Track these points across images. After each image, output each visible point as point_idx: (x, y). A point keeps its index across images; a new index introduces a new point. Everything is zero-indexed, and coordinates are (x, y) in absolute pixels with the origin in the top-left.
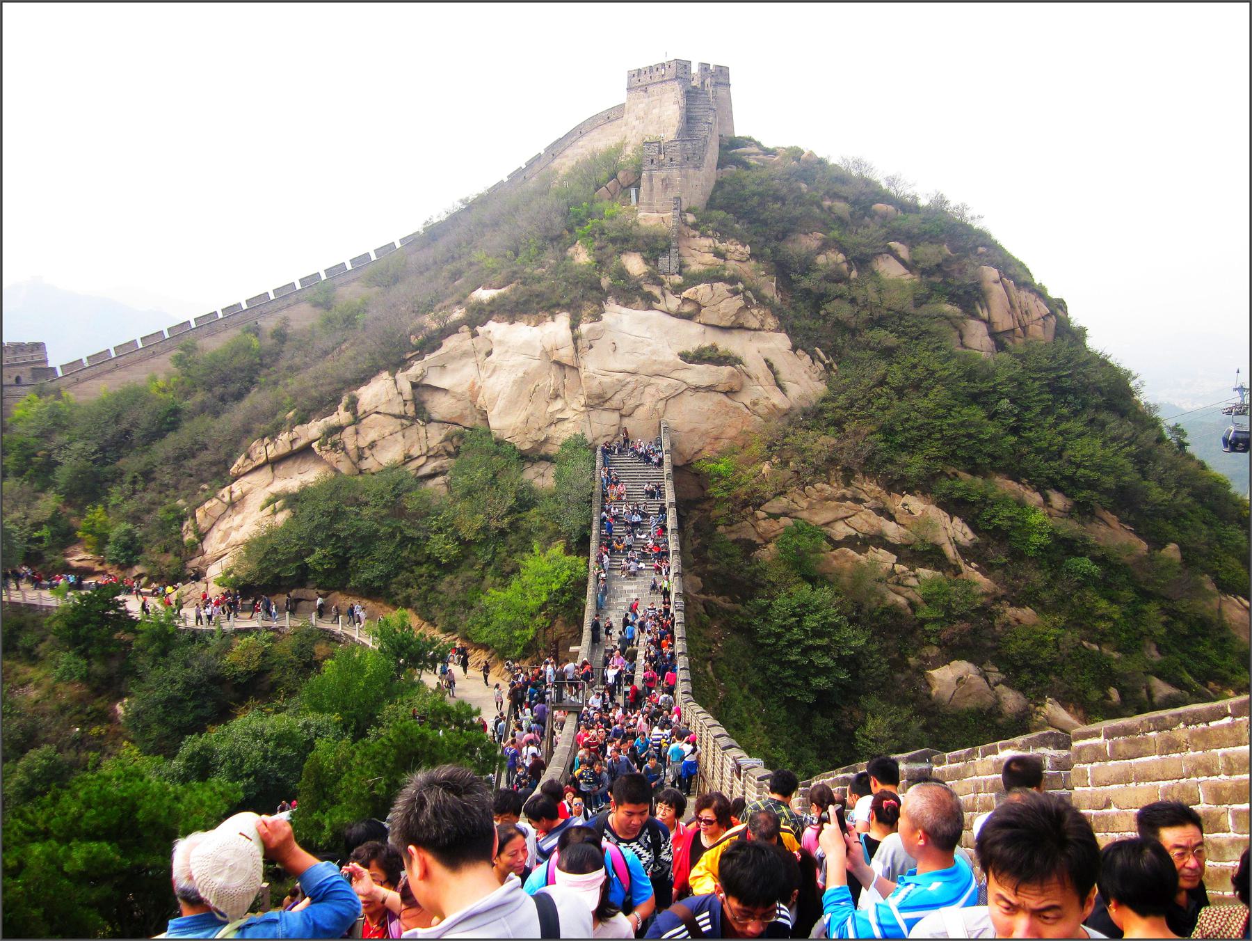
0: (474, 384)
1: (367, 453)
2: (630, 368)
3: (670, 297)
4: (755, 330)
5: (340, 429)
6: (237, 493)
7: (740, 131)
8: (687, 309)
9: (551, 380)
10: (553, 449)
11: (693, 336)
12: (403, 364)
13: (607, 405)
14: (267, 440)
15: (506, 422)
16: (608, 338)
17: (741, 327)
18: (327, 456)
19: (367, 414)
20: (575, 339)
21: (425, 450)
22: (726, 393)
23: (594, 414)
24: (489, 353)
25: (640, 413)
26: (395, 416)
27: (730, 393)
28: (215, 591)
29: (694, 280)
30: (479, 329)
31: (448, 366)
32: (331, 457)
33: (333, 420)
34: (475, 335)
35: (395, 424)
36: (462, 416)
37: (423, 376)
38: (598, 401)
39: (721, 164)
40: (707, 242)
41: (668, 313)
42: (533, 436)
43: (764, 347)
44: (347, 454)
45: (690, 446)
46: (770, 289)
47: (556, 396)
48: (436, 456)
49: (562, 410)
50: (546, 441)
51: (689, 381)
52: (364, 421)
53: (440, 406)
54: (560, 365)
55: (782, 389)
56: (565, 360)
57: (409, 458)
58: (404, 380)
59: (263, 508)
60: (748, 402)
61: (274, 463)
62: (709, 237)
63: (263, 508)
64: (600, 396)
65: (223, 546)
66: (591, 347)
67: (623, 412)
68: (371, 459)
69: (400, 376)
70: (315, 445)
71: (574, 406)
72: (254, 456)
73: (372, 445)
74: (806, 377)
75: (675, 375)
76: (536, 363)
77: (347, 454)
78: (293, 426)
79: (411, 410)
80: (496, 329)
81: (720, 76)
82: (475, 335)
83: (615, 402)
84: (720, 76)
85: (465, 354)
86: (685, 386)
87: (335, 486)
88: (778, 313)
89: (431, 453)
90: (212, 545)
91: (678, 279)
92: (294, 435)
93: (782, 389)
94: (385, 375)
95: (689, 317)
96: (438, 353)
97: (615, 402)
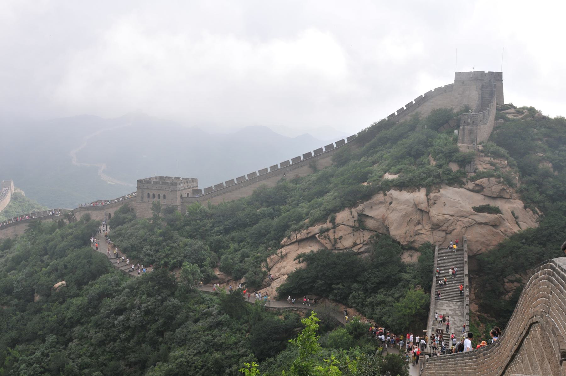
0: (384, 215)
1: (338, 241)
2: (451, 213)
3: (470, 183)
4: (508, 199)
5: (328, 230)
6: (284, 253)
8: (477, 188)
9: (416, 217)
10: (417, 245)
11: (479, 200)
12: (354, 205)
13: (441, 228)
14: (297, 232)
15: (396, 232)
16: (443, 199)
17: (501, 197)
18: (322, 241)
19: (339, 225)
20: (428, 200)
21: (362, 241)
22: (493, 226)
23: (434, 232)
24: (391, 203)
25: (454, 232)
26: (351, 226)
27: (495, 226)
28: (275, 293)
29: (481, 175)
30: (388, 193)
31: (374, 207)
32: (323, 241)
33: (325, 226)
34: (385, 195)
35: (350, 230)
36: (378, 228)
37: (363, 211)
38: (436, 227)
39: (497, 118)
40: (488, 159)
41: (469, 190)
42: (408, 239)
43: (512, 206)
44: (330, 241)
45: (476, 248)
46: (516, 178)
47: (419, 223)
48: (366, 244)
49: (421, 230)
50: (414, 241)
51: (477, 220)
52: (338, 228)
53: (370, 223)
54: (421, 211)
55: (519, 225)
56: (423, 209)
57: (355, 244)
59: (295, 260)
60: (503, 230)
61: (299, 242)
62: (488, 156)
63: (295, 260)
64: (437, 225)
65: (278, 274)
66: (435, 203)
67: (447, 232)
68: (339, 244)
69: (353, 210)
70: (317, 236)
71: (426, 228)
72: (292, 238)
73: (341, 238)
74: (530, 220)
75: (471, 217)
76: (411, 209)
77: (330, 241)
78: (308, 227)
79: (357, 225)
80: (394, 193)
82: (385, 195)
83: (444, 228)
84: (498, 76)
85: (381, 203)
86: (475, 222)
87: (323, 253)
88: (520, 191)
89: (365, 243)
90: (273, 273)
91: (473, 175)
92: (309, 231)
93: (519, 225)
94: (347, 209)
95: (477, 192)
96: (369, 201)
97: (444, 228)
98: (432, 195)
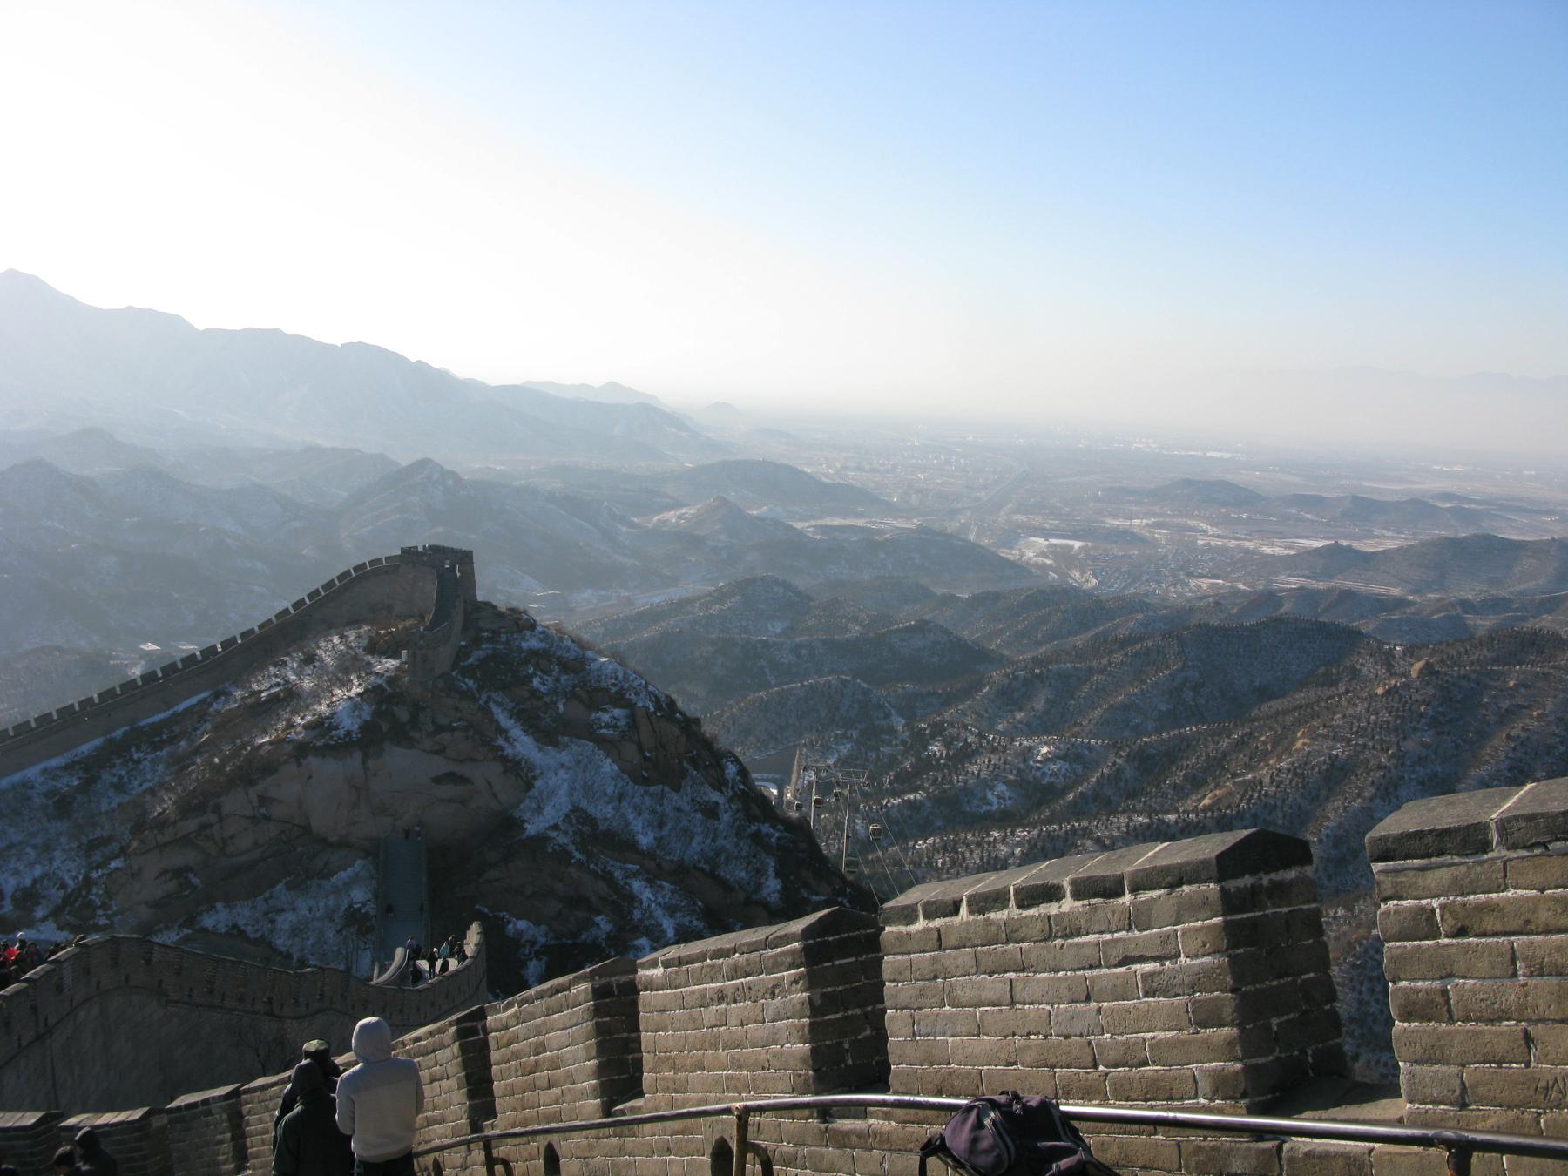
7: (481, 596)
11: (440, 765)
17: (472, 760)
29: (440, 729)
30: (303, 762)
34: (300, 765)
58: (253, 793)
73: (232, 837)
81: (465, 558)
82: (300, 765)
95: (437, 752)
98: (371, 763)
